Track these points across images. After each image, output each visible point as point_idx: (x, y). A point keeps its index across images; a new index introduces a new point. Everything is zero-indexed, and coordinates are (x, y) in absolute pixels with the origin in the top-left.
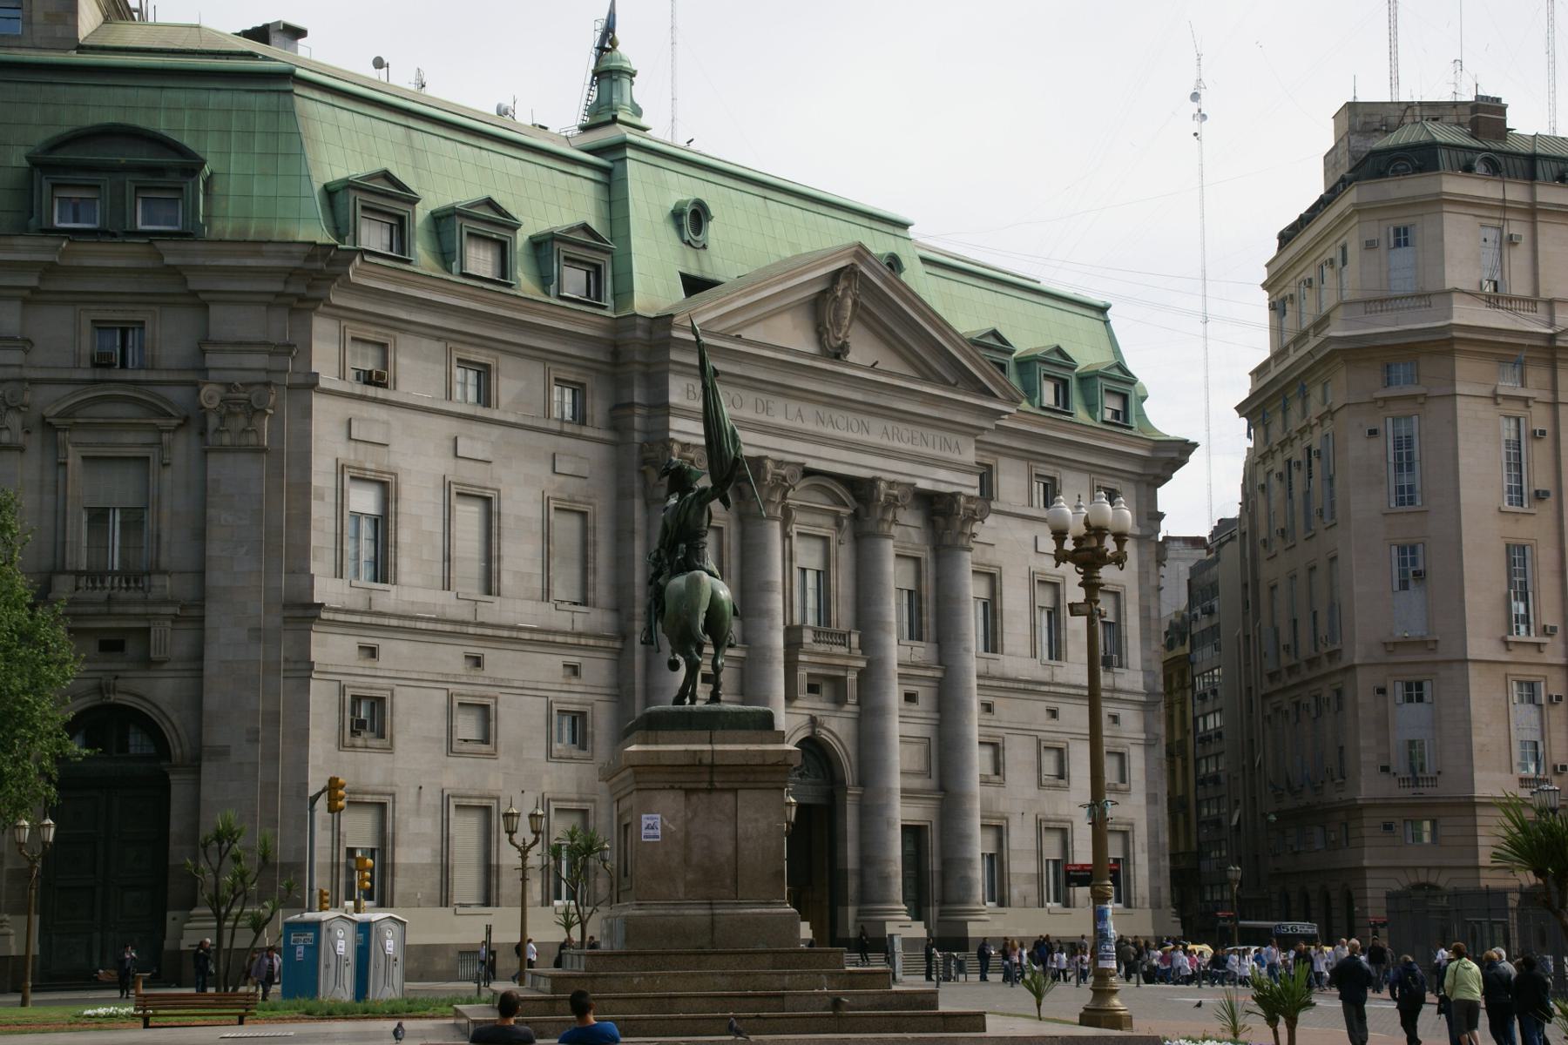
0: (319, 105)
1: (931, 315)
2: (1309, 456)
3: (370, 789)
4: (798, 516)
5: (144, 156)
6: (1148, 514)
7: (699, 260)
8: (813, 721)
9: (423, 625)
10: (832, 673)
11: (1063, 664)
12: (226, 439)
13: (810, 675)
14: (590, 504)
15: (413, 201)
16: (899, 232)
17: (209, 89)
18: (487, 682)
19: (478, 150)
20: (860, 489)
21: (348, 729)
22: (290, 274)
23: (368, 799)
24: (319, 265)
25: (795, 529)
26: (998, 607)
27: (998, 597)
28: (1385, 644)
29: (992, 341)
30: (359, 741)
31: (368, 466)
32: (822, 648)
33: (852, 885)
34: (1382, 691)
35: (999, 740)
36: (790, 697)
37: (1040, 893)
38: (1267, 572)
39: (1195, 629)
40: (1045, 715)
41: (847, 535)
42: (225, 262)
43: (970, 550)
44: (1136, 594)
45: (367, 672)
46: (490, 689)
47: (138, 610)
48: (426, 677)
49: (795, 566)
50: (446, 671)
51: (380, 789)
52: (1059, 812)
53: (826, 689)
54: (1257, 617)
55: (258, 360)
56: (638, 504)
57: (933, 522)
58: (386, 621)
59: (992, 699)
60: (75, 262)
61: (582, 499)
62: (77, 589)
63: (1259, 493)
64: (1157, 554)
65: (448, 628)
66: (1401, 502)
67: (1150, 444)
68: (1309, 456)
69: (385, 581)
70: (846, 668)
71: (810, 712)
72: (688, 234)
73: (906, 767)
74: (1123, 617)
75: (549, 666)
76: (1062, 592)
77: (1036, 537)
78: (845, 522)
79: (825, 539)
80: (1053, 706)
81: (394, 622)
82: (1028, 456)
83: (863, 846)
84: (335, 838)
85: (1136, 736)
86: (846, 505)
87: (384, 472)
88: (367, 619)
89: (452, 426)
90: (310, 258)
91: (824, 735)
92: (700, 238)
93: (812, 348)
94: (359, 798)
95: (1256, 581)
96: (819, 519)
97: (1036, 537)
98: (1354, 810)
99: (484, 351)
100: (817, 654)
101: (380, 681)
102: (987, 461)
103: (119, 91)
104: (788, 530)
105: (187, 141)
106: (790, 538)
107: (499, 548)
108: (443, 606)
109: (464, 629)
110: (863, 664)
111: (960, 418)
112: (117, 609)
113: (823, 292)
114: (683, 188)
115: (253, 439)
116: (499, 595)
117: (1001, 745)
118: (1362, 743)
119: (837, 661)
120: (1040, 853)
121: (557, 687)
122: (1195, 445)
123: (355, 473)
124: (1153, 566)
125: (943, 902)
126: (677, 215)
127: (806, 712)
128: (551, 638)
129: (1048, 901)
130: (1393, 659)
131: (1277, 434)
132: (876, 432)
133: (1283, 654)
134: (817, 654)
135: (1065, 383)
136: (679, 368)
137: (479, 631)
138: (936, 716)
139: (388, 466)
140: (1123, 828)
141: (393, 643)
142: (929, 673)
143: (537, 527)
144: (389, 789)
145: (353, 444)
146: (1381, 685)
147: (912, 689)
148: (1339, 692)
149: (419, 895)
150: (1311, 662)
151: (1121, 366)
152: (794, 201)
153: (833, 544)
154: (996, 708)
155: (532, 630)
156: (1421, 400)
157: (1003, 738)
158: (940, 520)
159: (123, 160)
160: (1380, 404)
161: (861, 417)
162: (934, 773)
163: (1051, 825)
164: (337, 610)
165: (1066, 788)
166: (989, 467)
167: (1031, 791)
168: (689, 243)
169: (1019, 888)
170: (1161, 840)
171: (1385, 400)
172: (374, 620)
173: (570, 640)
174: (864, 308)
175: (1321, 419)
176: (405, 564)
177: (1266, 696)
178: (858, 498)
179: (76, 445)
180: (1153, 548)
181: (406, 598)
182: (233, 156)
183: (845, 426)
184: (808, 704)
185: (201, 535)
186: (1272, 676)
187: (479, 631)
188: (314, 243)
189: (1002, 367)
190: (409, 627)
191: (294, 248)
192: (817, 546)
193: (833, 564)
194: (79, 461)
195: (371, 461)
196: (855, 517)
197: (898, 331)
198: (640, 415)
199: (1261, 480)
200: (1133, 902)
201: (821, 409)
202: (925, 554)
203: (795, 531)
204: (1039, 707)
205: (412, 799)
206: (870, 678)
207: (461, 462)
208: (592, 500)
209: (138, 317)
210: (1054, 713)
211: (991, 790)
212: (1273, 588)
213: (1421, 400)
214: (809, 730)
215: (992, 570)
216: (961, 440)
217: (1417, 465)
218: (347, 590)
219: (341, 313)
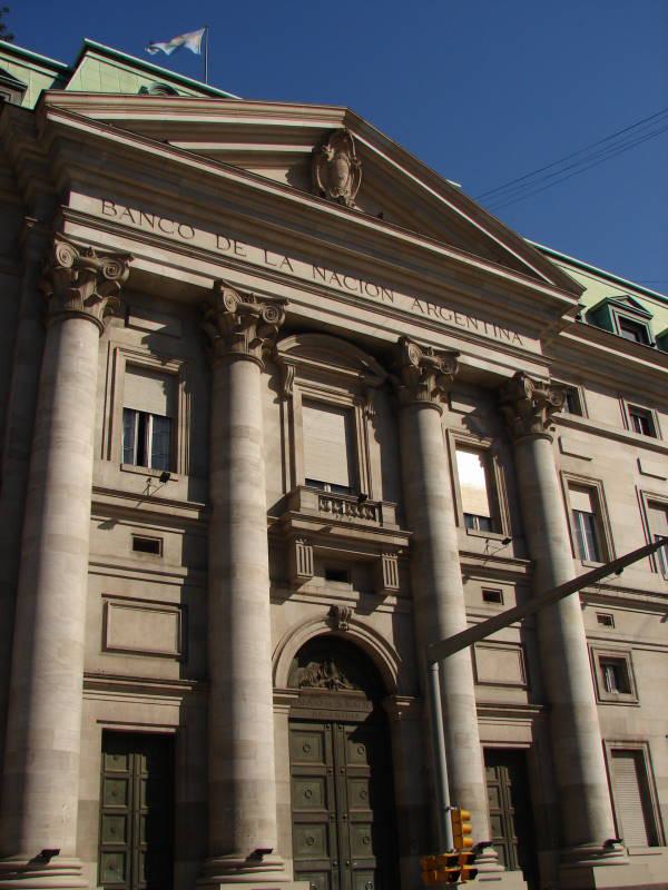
8: (335, 615)
20: (388, 356)
25: (297, 393)
35: (627, 656)
73: (492, 678)
77: (638, 461)
91: (354, 630)
97: (638, 461)
104: (287, 388)
106: (290, 398)
117: (628, 661)
142: (514, 568)
157: (630, 652)
158: (508, 410)
206: (419, 556)
215: (593, 483)
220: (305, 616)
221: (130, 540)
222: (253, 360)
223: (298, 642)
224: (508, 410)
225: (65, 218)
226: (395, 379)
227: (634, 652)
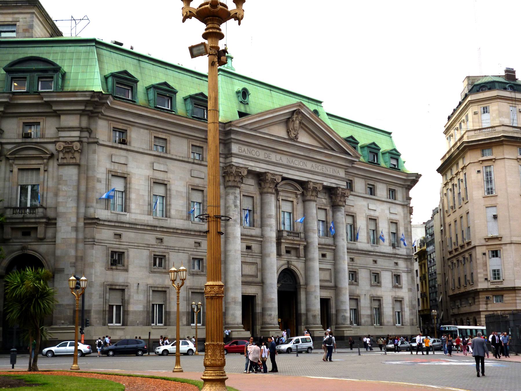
0: (105, 51)
1: (326, 126)
2: (459, 182)
3: (118, 284)
4: (281, 193)
5: (41, 66)
6: (406, 197)
7: (245, 107)
8: (288, 262)
9: (139, 227)
10: (294, 246)
11: (378, 245)
12: (65, 161)
13: (286, 247)
14: (205, 187)
15: (136, 81)
16: (319, 104)
17: (67, 46)
18: (165, 247)
19: (165, 69)
20: (303, 184)
21: (110, 263)
22: (86, 103)
23: (117, 287)
24: (96, 99)
25: (280, 198)
26: (355, 226)
27: (355, 223)
28: (485, 239)
29: (351, 140)
30: (114, 267)
31: (118, 171)
32: (290, 238)
33: (303, 318)
34: (484, 254)
35: (357, 271)
36: (279, 254)
37: (372, 321)
38: (448, 220)
39: (428, 241)
40: (372, 262)
41: (300, 200)
42: (63, 99)
43: (344, 206)
44: (403, 223)
45: (117, 243)
46: (166, 250)
47: (33, 220)
48: (141, 245)
49: (281, 210)
50: (149, 243)
51: (122, 284)
52: (378, 294)
53: (293, 252)
54: (445, 235)
55: (77, 134)
56: (222, 187)
58: (124, 225)
59: (353, 257)
60: (16, 102)
61: (202, 186)
62: (13, 213)
63: (445, 196)
64: (410, 211)
65: (149, 228)
66: (489, 193)
67: (406, 174)
68: (459, 182)
69: (125, 211)
70: (299, 245)
71: (287, 260)
72: (241, 99)
73: (322, 278)
74: (399, 230)
75: (190, 242)
76: (377, 222)
78: (299, 196)
79: (292, 202)
80: (375, 259)
81: (128, 225)
82: (364, 178)
83: (307, 305)
84: (105, 301)
85: (404, 269)
86: (299, 191)
87: (124, 174)
88: (117, 224)
89: (152, 159)
90: (92, 97)
91: (292, 267)
92: (246, 101)
93: (286, 137)
94: (114, 287)
95: (444, 223)
96: (290, 195)
98: (476, 293)
99: (164, 134)
100: (288, 240)
101: (123, 246)
102: (351, 179)
103: (38, 48)
104: (278, 198)
105: (58, 63)
106: (279, 201)
107: (170, 201)
108: (148, 221)
109: (155, 229)
110: (305, 243)
111: (339, 162)
112: (26, 221)
113: (289, 118)
114: (239, 85)
115: (74, 161)
116: (170, 217)
118: (479, 271)
119: (295, 242)
120: (371, 308)
121: (192, 250)
122: (421, 175)
123: (114, 174)
124: (409, 214)
125: (337, 324)
126: (238, 93)
127: (285, 260)
128: (189, 233)
129: (374, 323)
130: (488, 244)
131: (449, 176)
132: (309, 165)
133: (453, 245)
134: (288, 240)
135: (377, 154)
136: (235, 141)
137: (161, 229)
138: (333, 262)
139: (127, 172)
140: (400, 299)
141: (128, 233)
142: (330, 247)
143: (184, 195)
144: (126, 284)
145: (113, 163)
146: (484, 252)
147: (324, 252)
148: (471, 255)
149: (138, 322)
150: (462, 247)
151: (395, 150)
152: (281, 92)
153: (295, 203)
154: (355, 260)
155: (182, 230)
156: (494, 160)
158: (334, 197)
159: (34, 68)
160: (481, 162)
161: (303, 161)
162: (333, 281)
163: (375, 298)
164: (105, 221)
165: (380, 286)
166: (351, 181)
167: (368, 287)
168: (241, 102)
169: (363, 320)
170: (413, 303)
171: (483, 161)
172: (120, 225)
173: (197, 233)
174: (303, 124)
175: (463, 169)
176: (133, 206)
177: (449, 259)
178: (303, 188)
179: (16, 165)
180: (409, 209)
181: (133, 217)
182: (73, 67)
183: (297, 163)
184: (286, 257)
185: (56, 195)
186: (450, 253)
187: (161, 229)
188: (93, 91)
189: (355, 148)
190: (133, 226)
191: (87, 93)
192: (290, 204)
193: (295, 210)
194: (17, 170)
195: (120, 170)
196: (303, 194)
197: (316, 132)
198: (222, 157)
199: (445, 192)
200: (404, 324)
201: (289, 158)
203: (280, 197)
204: (370, 260)
205: (135, 288)
207: (155, 171)
208: (206, 186)
209: (38, 121)
210: (375, 262)
211: (353, 287)
212: (450, 225)
213: (494, 160)
214: (287, 266)
215: (353, 214)
216: (340, 170)
217: (493, 181)
218: (109, 214)
219: (108, 118)
220: (282, 264)
221: (245, 247)
222: (271, 193)
223: (280, 271)
224: (334, 197)
225: (232, 156)
226: (305, 192)
227: (359, 269)
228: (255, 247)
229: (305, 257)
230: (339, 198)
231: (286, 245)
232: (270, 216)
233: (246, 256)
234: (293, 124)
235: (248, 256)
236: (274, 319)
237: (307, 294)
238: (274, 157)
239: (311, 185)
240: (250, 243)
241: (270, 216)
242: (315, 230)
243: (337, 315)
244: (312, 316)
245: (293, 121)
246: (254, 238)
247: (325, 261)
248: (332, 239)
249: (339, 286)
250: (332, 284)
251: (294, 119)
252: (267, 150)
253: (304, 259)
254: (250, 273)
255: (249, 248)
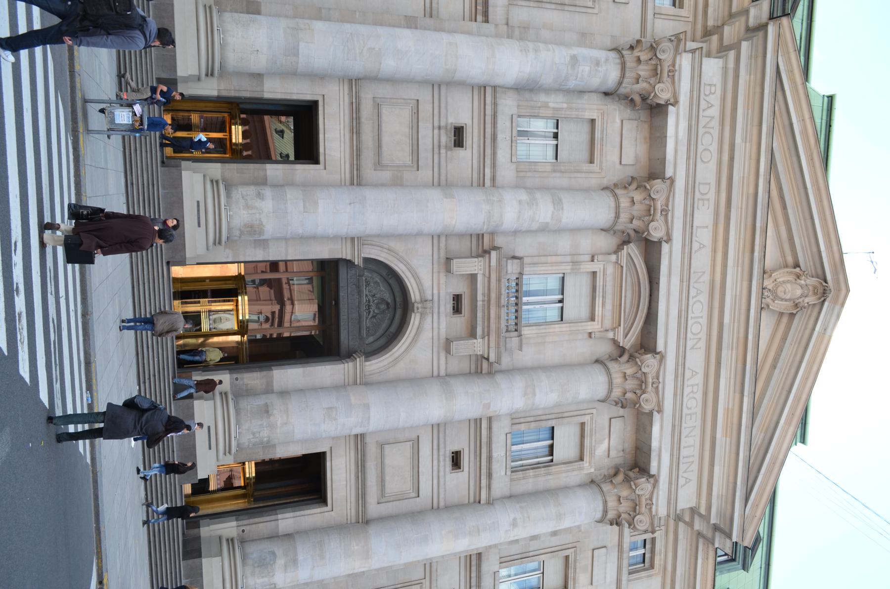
13: (473, 278)
53: (460, 322)
57: (616, 474)
79: (592, 319)
83: (301, 391)
86: (626, 336)
91: (415, 320)
104: (600, 257)
113: (797, 265)
127: (435, 292)
132: (696, 360)
136: (731, 64)
138: (442, 504)
158: (620, 477)
202: (588, 468)
214: (418, 298)
216: (692, 487)
228: (465, 157)
229: (446, 375)
230: (625, 493)
231: (480, 278)
232: (558, 203)
233: (436, 124)
234: (788, 281)
235: (436, 131)
236: (247, 207)
237: (339, 388)
238: (704, 217)
239: (649, 362)
240: (471, 137)
241: (558, 203)
242: (534, 394)
243: (274, 537)
244: (266, 405)
245: (798, 277)
246: (488, 151)
247: (442, 463)
248: (508, 493)
249: (372, 529)
250: (374, 509)
251: (803, 282)
252: (718, 191)
253: (443, 373)
254: (385, 139)
255: (458, 136)
